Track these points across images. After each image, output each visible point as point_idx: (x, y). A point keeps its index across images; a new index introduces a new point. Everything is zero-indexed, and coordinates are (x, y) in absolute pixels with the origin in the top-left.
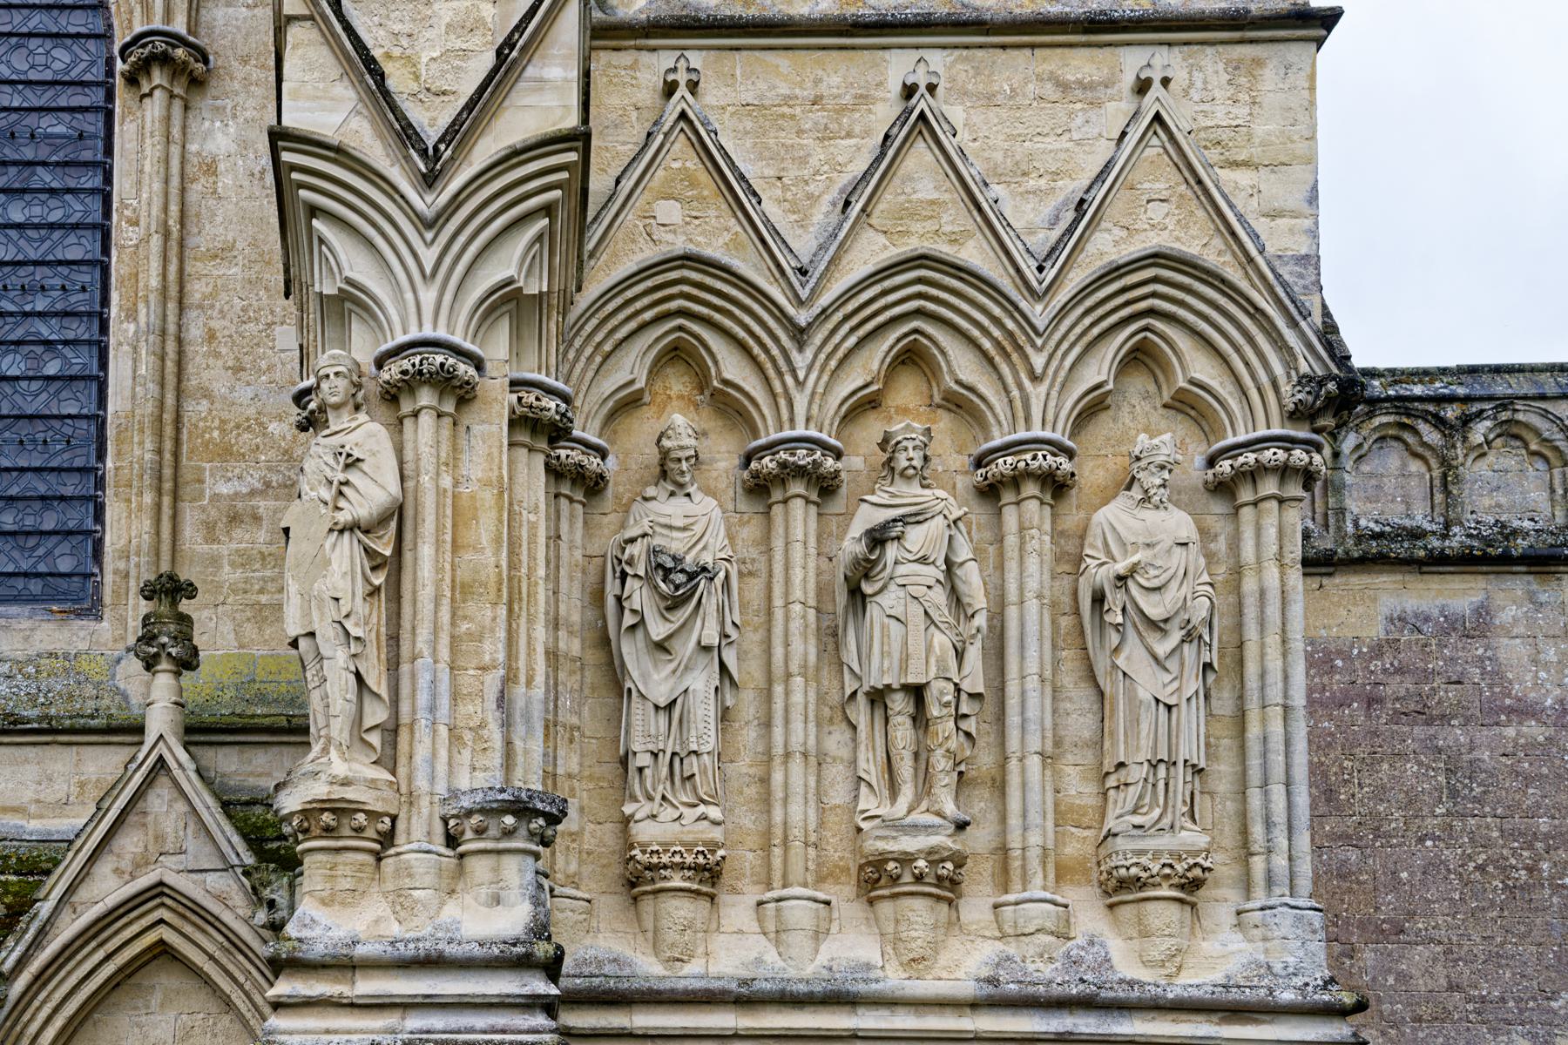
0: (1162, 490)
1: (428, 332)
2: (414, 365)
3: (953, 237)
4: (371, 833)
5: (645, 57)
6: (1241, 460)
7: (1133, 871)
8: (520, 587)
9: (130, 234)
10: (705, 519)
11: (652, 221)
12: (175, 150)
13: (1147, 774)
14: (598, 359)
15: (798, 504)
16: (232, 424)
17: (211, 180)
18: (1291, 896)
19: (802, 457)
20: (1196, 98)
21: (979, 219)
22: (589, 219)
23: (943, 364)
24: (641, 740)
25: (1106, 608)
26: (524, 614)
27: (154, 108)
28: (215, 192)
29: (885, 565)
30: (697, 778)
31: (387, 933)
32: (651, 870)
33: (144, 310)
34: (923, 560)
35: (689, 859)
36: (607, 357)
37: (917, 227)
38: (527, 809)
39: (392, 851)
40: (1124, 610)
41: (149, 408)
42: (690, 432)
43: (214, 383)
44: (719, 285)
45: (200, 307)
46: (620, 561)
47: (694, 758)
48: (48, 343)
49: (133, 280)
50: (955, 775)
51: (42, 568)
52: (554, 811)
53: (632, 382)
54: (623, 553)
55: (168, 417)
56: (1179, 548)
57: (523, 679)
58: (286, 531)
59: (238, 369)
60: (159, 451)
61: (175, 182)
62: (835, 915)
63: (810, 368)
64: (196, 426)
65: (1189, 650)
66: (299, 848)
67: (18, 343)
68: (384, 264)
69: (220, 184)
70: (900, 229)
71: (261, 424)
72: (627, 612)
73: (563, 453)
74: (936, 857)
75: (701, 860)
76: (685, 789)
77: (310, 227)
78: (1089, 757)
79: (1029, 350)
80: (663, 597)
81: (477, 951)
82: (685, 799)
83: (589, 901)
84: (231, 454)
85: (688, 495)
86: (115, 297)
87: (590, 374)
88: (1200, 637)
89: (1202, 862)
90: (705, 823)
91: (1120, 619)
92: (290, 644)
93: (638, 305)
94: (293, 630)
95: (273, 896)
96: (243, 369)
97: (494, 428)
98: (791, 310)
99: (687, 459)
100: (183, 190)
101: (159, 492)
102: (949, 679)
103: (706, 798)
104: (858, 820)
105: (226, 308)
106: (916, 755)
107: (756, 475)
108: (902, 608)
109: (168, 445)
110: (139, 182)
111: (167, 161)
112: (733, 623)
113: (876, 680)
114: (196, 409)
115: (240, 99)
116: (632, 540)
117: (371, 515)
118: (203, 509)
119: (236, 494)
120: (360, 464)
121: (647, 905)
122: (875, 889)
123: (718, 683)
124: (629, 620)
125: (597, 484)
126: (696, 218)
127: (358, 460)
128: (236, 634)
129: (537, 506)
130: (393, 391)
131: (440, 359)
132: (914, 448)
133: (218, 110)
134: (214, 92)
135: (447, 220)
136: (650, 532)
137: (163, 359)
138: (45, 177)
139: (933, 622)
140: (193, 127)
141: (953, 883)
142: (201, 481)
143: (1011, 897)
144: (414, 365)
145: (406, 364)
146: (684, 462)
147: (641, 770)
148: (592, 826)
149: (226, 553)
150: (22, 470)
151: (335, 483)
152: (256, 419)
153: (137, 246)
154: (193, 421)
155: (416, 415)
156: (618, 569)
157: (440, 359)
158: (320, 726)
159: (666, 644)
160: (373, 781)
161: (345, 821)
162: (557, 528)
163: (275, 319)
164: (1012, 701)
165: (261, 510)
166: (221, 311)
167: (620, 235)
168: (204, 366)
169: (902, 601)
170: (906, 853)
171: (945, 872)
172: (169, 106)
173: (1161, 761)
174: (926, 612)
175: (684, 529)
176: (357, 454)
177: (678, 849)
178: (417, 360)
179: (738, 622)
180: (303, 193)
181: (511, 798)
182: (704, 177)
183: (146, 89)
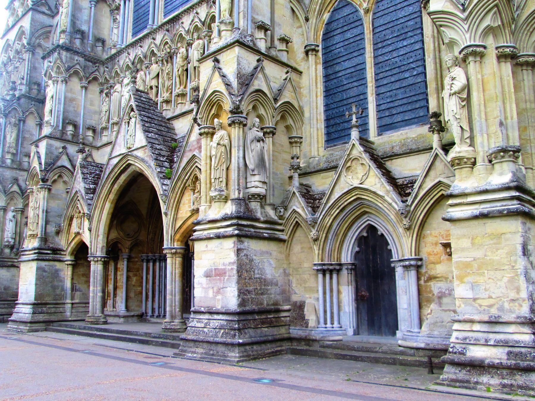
1: (469, 44)
14: (529, 34)
36: (531, 33)
48: (413, 68)
51: (417, 116)
67: (408, 70)
73: (521, 59)
81: (496, 187)
86: (426, 54)
87: (527, 38)
131: (471, 49)
138: (410, 34)
150: (411, 96)
157: (471, 49)
176: (454, 76)
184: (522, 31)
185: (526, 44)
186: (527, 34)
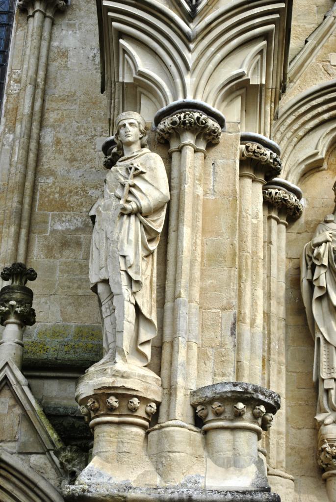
2: (180, 118)
4: (141, 412)
8: (246, 262)
9: (15, 87)
11: (328, 63)
12: (45, 44)
14: (295, 140)
16: (67, 191)
17: (64, 60)
22: (289, 60)
26: (249, 279)
27: (35, 22)
28: (66, 66)
31: (152, 482)
33: (19, 126)
38: (253, 398)
39: (157, 427)
41: (18, 178)
43: (58, 168)
45: (53, 126)
46: (311, 258)
49: (14, 112)
52: (271, 402)
54: (313, 253)
55: (28, 185)
57: (248, 321)
58: (93, 218)
59: (73, 160)
60: (21, 203)
61: (43, 60)
64: (45, 191)
66: (92, 422)
68: (163, 65)
69: (69, 62)
71: (84, 191)
72: (316, 289)
73: (273, 191)
77: (118, 43)
84: (65, 207)
92: (92, 289)
93: (320, 109)
94: (94, 279)
95: (74, 469)
96: (76, 160)
97: (230, 162)
100: (47, 65)
101: (20, 227)
105: (68, 127)
109: (27, 200)
110: (23, 61)
111: (39, 48)
114: (44, 182)
115: (84, 20)
116: (319, 245)
117: (149, 205)
118: (46, 238)
119: (67, 230)
120: (143, 175)
124: (317, 293)
125: (295, 213)
127: (142, 173)
128: (62, 313)
129: (257, 214)
130: (166, 136)
133: (70, 26)
134: (69, 16)
135: (203, 38)
137: (28, 152)
140: (56, 32)
142: (46, 222)
144: (180, 118)
145: (175, 118)
149: (58, 264)
151: (127, 187)
152: (82, 188)
153: (18, 94)
154: (44, 188)
155: (180, 150)
156: (310, 264)
158: (109, 342)
160: (144, 376)
161: (124, 403)
162: (270, 237)
163: (96, 134)
165: (82, 240)
166: (65, 128)
167: (308, 70)
168: (53, 158)
172: (43, 22)
178: (182, 115)
180: (114, 24)
181: (241, 390)
183: (31, 13)
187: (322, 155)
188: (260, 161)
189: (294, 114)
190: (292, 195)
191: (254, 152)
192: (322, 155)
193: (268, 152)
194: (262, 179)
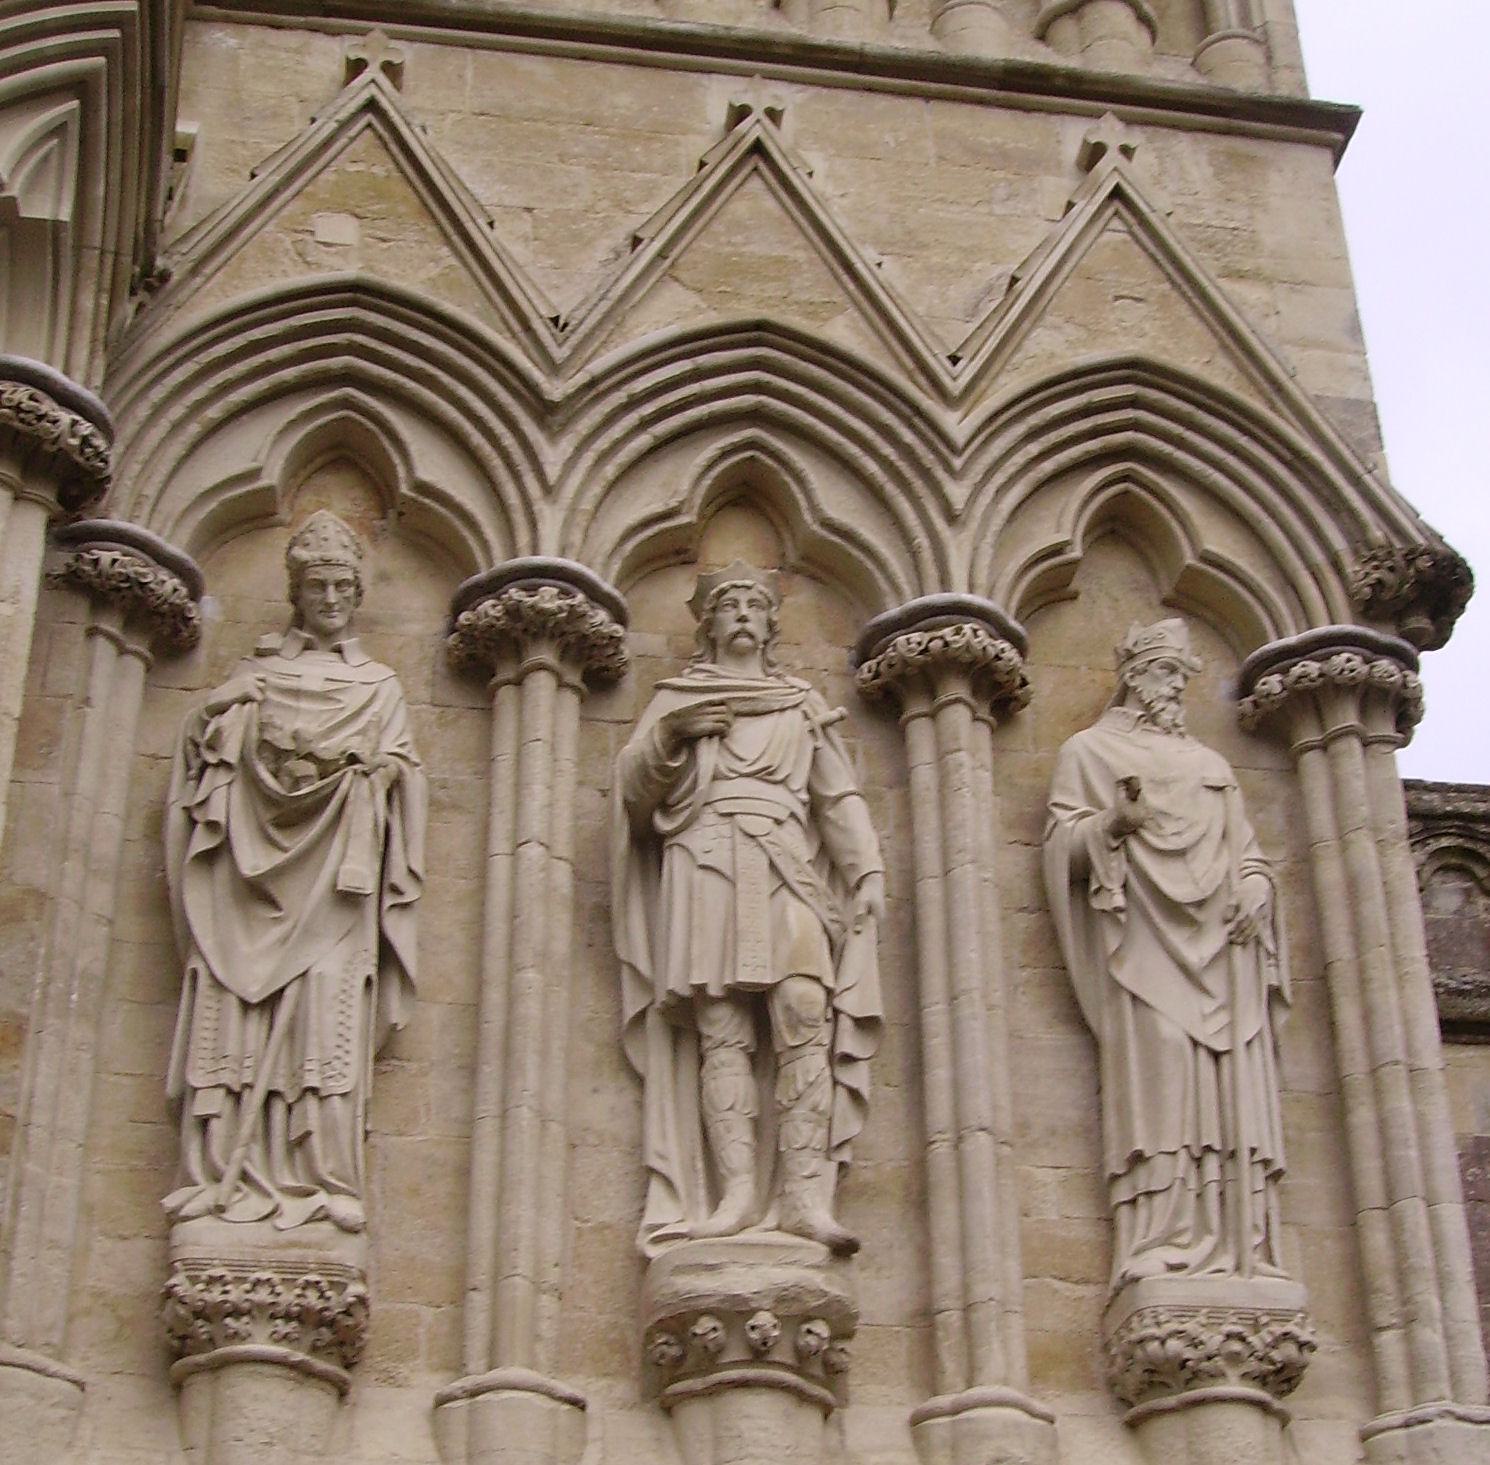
0: (1173, 706)
3: (811, 308)
5: (321, 41)
6: (1296, 670)
7: (1174, 1345)
10: (369, 691)
11: (307, 237)
13: (1187, 1171)
14: (194, 429)
15: (542, 685)
18: (1455, 1400)
19: (548, 598)
20: (1172, 187)
21: (851, 286)
23: (800, 497)
24: (210, 1065)
25: (1094, 887)
29: (695, 782)
30: (316, 1141)
32: (208, 1319)
34: (765, 775)
35: (288, 1297)
37: (753, 289)
40: (1125, 886)
42: (346, 540)
44: (415, 335)
47: (311, 1103)
50: (833, 1167)
53: (254, 474)
54: (203, 732)
56: (1210, 795)
62: (594, 1430)
63: (570, 463)
65: (1241, 958)
70: (722, 288)
73: (106, 557)
74: (795, 1308)
75: (312, 1299)
76: (292, 1166)
78: (1073, 1154)
79: (940, 473)
80: (269, 799)
82: (290, 1182)
83: (80, 1385)
85: (339, 650)
87: (177, 449)
88: (1258, 942)
89: (1296, 1330)
90: (327, 1226)
91: (1119, 900)
93: (273, 354)
98: (538, 375)
99: (339, 584)
102: (817, 980)
103: (333, 1180)
104: (643, 1242)
106: (757, 1125)
107: (469, 635)
108: (727, 855)
112: (411, 872)
113: (676, 980)
116: (221, 710)
121: (199, 1392)
122: (678, 1379)
123: (372, 971)
124: (202, 842)
126: (384, 240)
132: (751, 603)
136: (259, 696)
139: (785, 884)
141: (833, 1373)
143: (944, 1401)
146: (331, 589)
147: (204, 1122)
148: (108, 1244)
159: (274, 889)
164: (935, 1041)
169: (727, 842)
170: (736, 1298)
171: (812, 1340)
173: (1208, 1149)
174: (772, 866)
175: (325, 696)
177: (264, 1275)
179: (418, 868)
182: (401, 189)
184: (157, 394)
185: (158, 478)
186: (177, 426)
187: (272, 477)
188: (38, 441)
189: (195, 359)
190: (163, 574)
191: (18, 408)
192: (272, 477)
193: (66, 417)
194: (50, 496)
